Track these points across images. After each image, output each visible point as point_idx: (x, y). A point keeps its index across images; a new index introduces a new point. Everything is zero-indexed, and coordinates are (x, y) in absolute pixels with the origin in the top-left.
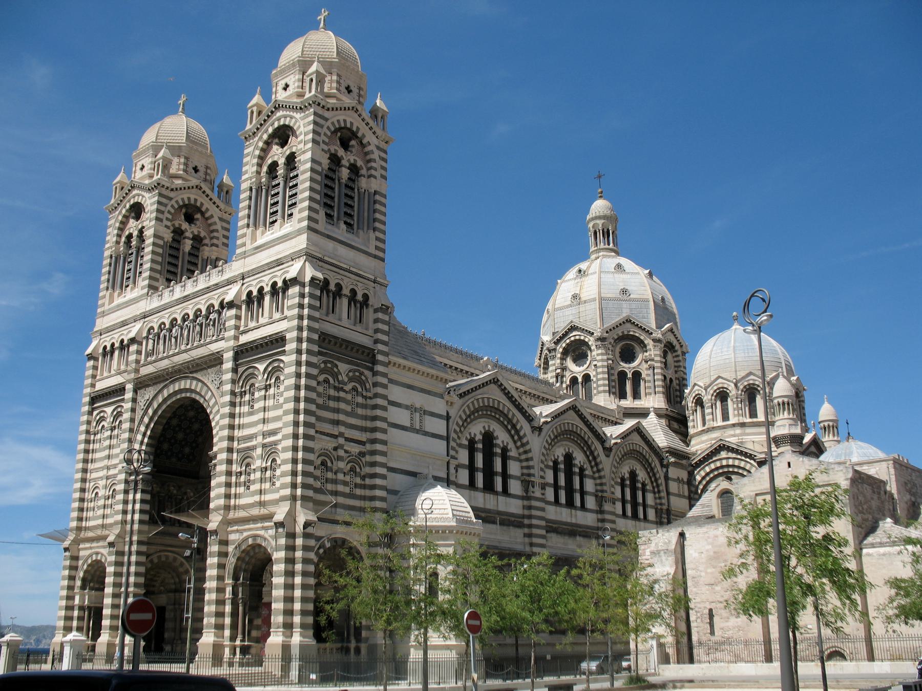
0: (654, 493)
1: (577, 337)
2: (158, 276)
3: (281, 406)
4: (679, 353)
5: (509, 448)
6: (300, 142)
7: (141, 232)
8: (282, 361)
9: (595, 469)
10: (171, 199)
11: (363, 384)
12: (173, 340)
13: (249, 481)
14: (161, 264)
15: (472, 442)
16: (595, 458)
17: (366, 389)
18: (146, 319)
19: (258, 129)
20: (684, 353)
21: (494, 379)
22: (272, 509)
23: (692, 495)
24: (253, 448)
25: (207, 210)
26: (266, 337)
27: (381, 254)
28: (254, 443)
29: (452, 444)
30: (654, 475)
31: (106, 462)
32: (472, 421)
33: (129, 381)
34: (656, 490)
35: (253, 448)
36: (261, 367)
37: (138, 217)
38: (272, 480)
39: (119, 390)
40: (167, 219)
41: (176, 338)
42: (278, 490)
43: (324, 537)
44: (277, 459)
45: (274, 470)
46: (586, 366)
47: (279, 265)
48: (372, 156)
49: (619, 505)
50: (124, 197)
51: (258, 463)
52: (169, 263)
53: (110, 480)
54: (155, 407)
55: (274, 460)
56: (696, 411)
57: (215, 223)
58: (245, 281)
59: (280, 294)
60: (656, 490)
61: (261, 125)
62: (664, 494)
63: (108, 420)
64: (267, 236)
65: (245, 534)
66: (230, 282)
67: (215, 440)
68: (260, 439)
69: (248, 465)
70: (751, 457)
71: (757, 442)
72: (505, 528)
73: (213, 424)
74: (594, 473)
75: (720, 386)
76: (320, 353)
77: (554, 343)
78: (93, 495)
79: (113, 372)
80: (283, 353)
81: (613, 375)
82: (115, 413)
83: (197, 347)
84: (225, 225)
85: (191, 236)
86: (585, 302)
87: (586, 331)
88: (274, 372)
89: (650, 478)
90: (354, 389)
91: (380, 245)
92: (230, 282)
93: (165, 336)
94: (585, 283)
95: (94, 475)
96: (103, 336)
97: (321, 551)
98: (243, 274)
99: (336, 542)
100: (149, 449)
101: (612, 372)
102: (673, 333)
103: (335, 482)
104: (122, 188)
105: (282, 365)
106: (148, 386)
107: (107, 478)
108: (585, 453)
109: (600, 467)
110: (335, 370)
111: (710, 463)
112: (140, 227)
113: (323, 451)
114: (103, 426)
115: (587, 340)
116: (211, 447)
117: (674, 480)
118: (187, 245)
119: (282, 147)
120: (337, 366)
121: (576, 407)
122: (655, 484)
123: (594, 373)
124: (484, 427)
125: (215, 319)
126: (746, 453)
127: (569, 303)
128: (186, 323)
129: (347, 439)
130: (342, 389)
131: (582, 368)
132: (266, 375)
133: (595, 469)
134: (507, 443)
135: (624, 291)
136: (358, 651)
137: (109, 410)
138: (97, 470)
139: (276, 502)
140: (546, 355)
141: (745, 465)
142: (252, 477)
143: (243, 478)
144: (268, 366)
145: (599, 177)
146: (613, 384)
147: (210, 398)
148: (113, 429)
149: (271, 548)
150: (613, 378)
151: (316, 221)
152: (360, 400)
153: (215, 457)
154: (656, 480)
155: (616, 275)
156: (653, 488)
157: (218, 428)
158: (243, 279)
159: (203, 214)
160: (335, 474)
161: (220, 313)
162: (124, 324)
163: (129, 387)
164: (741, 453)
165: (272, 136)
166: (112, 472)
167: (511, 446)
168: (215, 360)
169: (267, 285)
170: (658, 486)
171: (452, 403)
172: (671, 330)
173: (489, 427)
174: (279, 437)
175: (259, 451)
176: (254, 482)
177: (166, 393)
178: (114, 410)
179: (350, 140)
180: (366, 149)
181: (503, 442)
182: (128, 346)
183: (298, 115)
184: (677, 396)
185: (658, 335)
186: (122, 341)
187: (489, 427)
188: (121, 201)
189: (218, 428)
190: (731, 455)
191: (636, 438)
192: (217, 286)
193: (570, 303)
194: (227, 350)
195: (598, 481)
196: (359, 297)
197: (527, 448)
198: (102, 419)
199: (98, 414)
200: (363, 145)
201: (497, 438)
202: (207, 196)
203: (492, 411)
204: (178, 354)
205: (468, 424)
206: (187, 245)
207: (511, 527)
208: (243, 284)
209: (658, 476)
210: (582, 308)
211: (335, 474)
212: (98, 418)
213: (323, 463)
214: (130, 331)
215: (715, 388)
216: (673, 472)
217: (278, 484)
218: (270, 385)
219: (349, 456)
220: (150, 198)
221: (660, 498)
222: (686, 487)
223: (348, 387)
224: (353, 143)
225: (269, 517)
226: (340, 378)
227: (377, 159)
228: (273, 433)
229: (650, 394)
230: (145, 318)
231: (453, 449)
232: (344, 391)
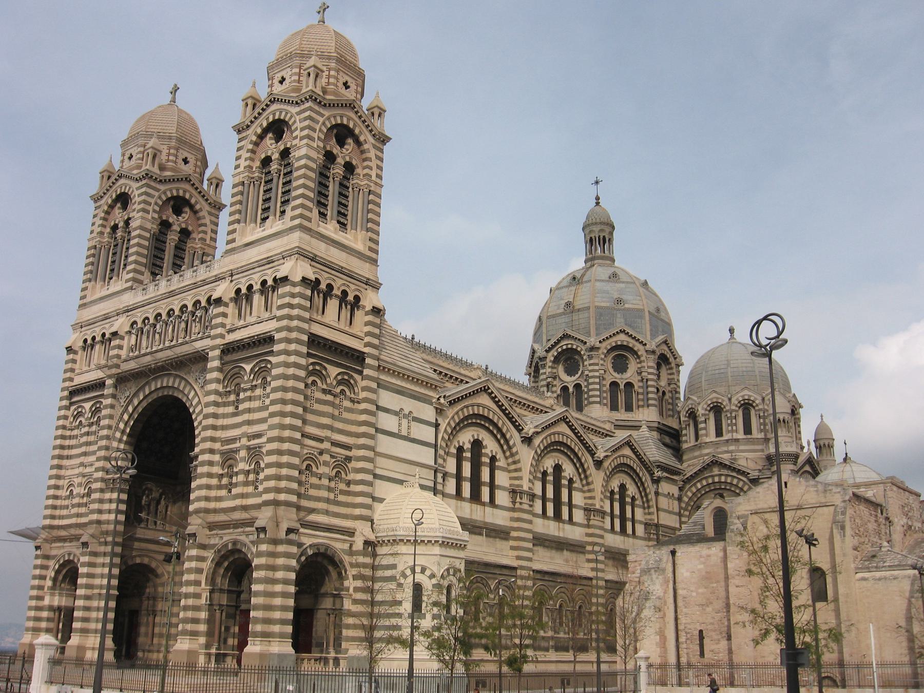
0: (644, 508)
1: (569, 346)
2: (143, 269)
3: (266, 408)
4: (673, 365)
5: (498, 457)
6: (296, 137)
7: (127, 222)
8: (270, 362)
9: (584, 482)
10: (158, 190)
11: (351, 387)
12: (157, 336)
13: (231, 484)
14: (146, 257)
15: (460, 449)
16: (584, 471)
17: (354, 393)
18: (129, 313)
19: (252, 122)
20: (678, 366)
21: (484, 387)
22: (254, 513)
23: (682, 511)
24: (237, 451)
25: (196, 203)
26: (254, 336)
27: (374, 256)
28: (237, 445)
29: (441, 452)
30: (645, 489)
32: (461, 429)
33: (110, 377)
34: (646, 505)
35: (237, 451)
36: (248, 367)
37: (125, 207)
38: (255, 484)
39: (100, 385)
40: (154, 211)
41: (160, 334)
42: (260, 494)
43: (305, 544)
44: (261, 462)
45: (258, 474)
46: (577, 376)
47: (269, 263)
48: (368, 155)
49: (608, 520)
50: (110, 187)
51: (242, 466)
52: (155, 256)
53: (86, 478)
54: (136, 405)
56: (689, 425)
57: (204, 218)
58: (234, 277)
59: (270, 292)
60: (646, 505)
61: (255, 118)
62: (654, 510)
64: (258, 233)
65: (225, 539)
66: (218, 279)
67: (197, 441)
68: (244, 441)
69: (231, 466)
70: (744, 473)
71: (750, 459)
72: (491, 539)
73: (196, 424)
74: (583, 486)
75: (715, 400)
76: (309, 355)
77: (546, 351)
78: (68, 493)
79: (93, 366)
80: (271, 353)
81: (604, 385)
82: (93, 409)
83: (182, 344)
84: (213, 219)
85: (179, 229)
86: (579, 310)
87: (579, 340)
88: (262, 372)
89: (640, 493)
90: (342, 391)
91: (373, 246)
92: (218, 279)
93: (148, 332)
94: (580, 291)
96: (83, 329)
97: (303, 558)
98: (231, 270)
99: (318, 549)
100: (127, 447)
101: (604, 383)
102: (667, 344)
103: (318, 487)
104: (109, 177)
105: (269, 366)
106: (129, 380)
108: (575, 465)
109: (590, 479)
110: (324, 372)
111: (702, 479)
112: (126, 218)
113: (308, 455)
115: (579, 349)
116: (192, 446)
117: (665, 496)
118: (173, 237)
119: (277, 142)
120: (326, 369)
121: (567, 418)
122: (645, 499)
123: (586, 384)
124: (473, 436)
125: (201, 317)
126: (739, 470)
127: (562, 310)
128: (171, 319)
129: (335, 444)
130: (330, 392)
131: (573, 378)
132: (252, 376)
133: (584, 482)
134: (496, 453)
135: (619, 301)
136: (337, 661)
137: (87, 405)
139: (258, 507)
140: (537, 363)
141: (738, 483)
142: (234, 480)
144: (254, 366)
145: (597, 182)
146: (605, 395)
147: (194, 398)
149: (252, 553)
150: (605, 389)
151: (309, 220)
152: (347, 403)
153: (196, 457)
154: (646, 495)
155: (611, 284)
156: (643, 503)
157: (200, 428)
158: (232, 275)
159: (192, 207)
160: (320, 479)
161: (207, 310)
162: (106, 317)
163: (109, 382)
164: (734, 470)
165: (266, 131)
166: (88, 470)
167: (500, 456)
168: (201, 358)
169: (256, 283)
170: (648, 501)
171: (441, 410)
172: (665, 342)
173: (478, 435)
174: (264, 439)
175: (243, 453)
176: (236, 485)
178: (92, 406)
179: (346, 137)
180: (362, 148)
181: (492, 451)
182: (110, 340)
183: (294, 110)
184: (669, 410)
185: (652, 346)
186: (104, 335)
187: (478, 435)
188: (108, 190)
189: (200, 428)
190: (725, 472)
191: (627, 451)
192: (205, 283)
193: (562, 310)
194: (213, 348)
195: (588, 495)
196: (350, 298)
197: (517, 458)
198: (80, 414)
199: (75, 410)
200: (358, 143)
201: (486, 447)
202: (197, 188)
203: (479, 420)
204: (161, 350)
205: (457, 432)
206: (173, 237)
207: (498, 539)
208: (232, 281)
209: (648, 491)
210: (575, 317)
211: (320, 479)
213: (308, 467)
214: (112, 325)
215: (709, 402)
216: (665, 487)
217: (261, 488)
218: (256, 386)
219: (335, 462)
220: (138, 189)
221: (649, 514)
222: (676, 502)
223: (338, 390)
224: (350, 141)
225: (250, 523)
226: (329, 381)
227: (373, 158)
228: (258, 436)
229: (643, 406)
231: (441, 457)
232: (332, 394)
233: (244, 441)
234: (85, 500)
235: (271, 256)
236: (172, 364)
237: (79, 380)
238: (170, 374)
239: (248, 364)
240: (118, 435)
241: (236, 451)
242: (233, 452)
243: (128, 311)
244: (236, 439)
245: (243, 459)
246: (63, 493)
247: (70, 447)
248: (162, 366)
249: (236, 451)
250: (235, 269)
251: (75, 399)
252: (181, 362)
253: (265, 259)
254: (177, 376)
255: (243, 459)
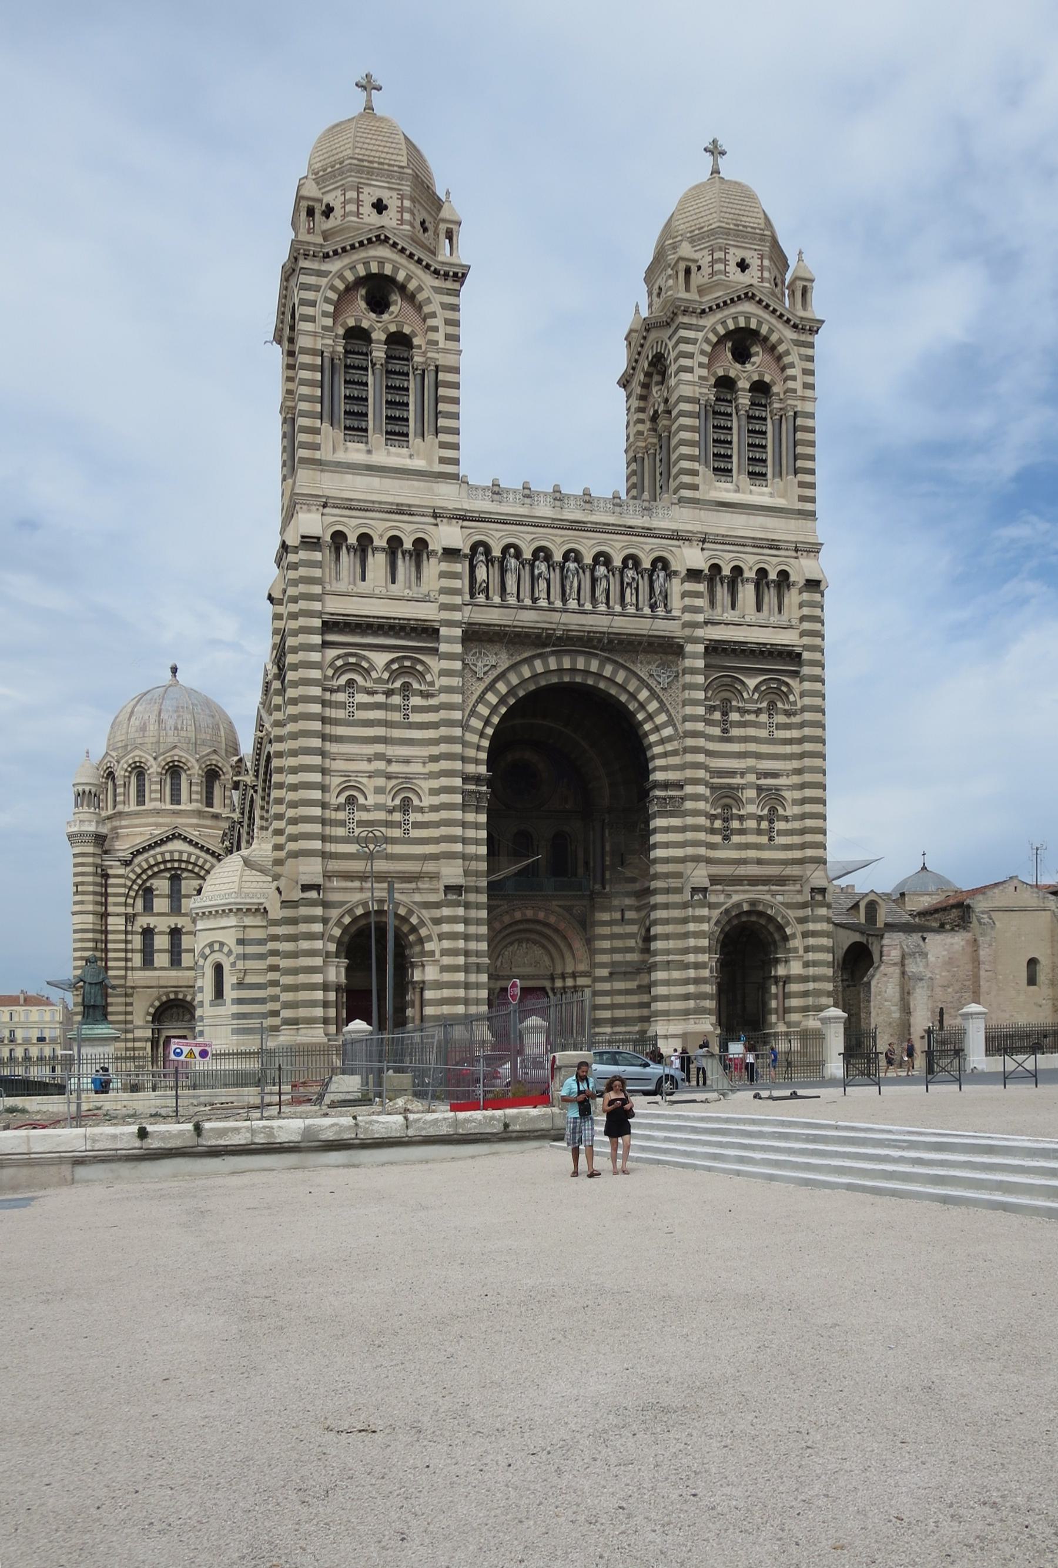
12: (542, 585)
13: (727, 829)
18: (466, 523)
24: (743, 787)
28: (737, 780)
31: (380, 748)
35: (743, 787)
36: (752, 682)
51: (751, 809)
53: (394, 782)
55: (773, 810)
58: (706, 545)
63: (374, 675)
69: (729, 807)
78: (342, 799)
82: (395, 666)
95: (338, 765)
96: (327, 510)
98: (706, 534)
107: (389, 777)
114: (351, 683)
137: (380, 659)
138: (349, 758)
142: (735, 824)
143: (718, 824)
144: (761, 683)
148: (389, 693)
158: (704, 541)
175: (751, 793)
177: (539, 667)
178: (393, 661)
199: (339, 657)
212: (339, 663)
230: (464, 520)
233: (751, 778)
234: (397, 816)
235: (779, 541)
236: (600, 640)
237: (335, 606)
238: (596, 655)
239: (749, 677)
240: (476, 723)
241: (738, 789)
242: (733, 789)
243: (464, 518)
244: (735, 773)
245: (750, 801)
246: (334, 800)
247: (336, 722)
248: (590, 640)
249: (738, 789)
250: (711, 534)
251: (331, 638)
252: (631, 643)
253: (768, 540)
254: (608, 659)
255: (750, 801)
